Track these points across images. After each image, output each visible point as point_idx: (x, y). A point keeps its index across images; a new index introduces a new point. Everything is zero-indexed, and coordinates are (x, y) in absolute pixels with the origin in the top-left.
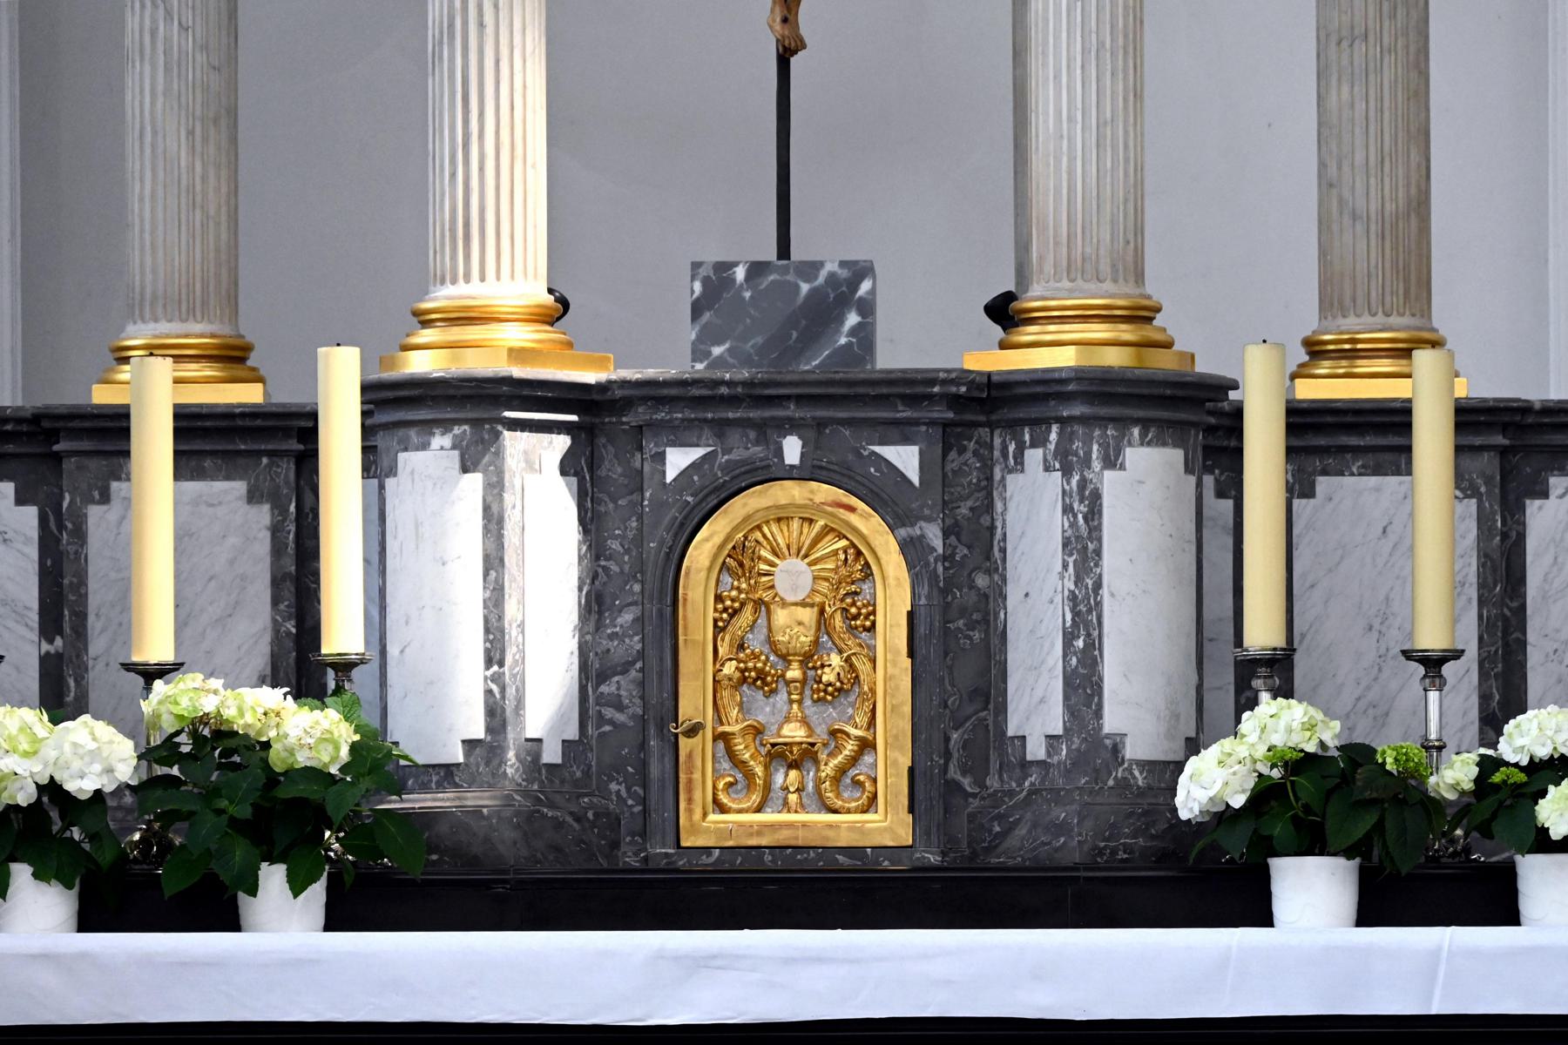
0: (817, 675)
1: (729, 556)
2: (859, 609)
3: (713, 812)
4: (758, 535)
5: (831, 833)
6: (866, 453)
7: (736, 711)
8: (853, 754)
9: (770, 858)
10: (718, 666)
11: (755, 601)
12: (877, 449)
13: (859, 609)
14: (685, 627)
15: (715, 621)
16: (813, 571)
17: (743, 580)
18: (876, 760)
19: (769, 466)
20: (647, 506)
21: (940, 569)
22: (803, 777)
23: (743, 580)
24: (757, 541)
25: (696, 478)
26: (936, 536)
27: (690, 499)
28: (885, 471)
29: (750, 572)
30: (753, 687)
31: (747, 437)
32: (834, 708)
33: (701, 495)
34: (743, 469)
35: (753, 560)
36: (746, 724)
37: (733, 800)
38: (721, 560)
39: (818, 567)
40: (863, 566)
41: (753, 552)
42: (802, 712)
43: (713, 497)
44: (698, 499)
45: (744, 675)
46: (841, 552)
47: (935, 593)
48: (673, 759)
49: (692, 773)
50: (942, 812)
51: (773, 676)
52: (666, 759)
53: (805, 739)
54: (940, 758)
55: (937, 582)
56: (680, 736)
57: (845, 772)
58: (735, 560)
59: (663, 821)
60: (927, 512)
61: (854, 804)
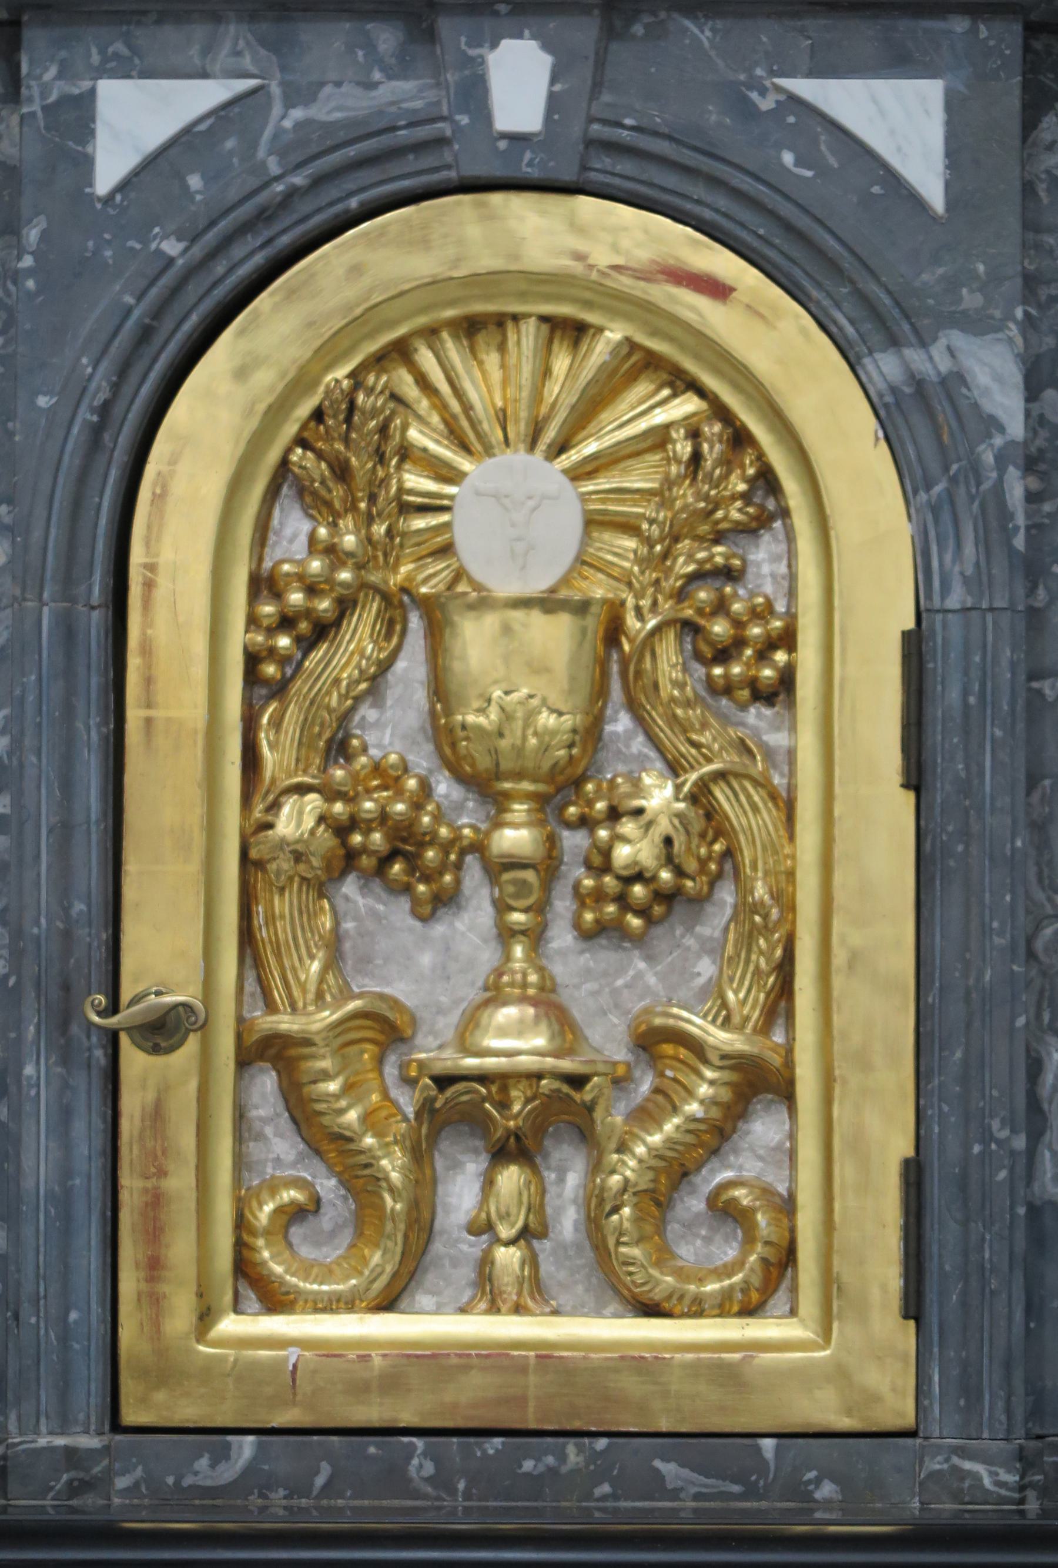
0: (595, 845)
1: (301, 442)
2: (738, 624)
3: (237, 1310)
4: (405, 383)
5: (631, 1385)
6: (766, 104)
7: (315, 966)
8: (715, 1113)
9: (429, 1468)
10: (258, 812)
11: (386, 597)
12: (804, 87)
13: (738, 624)
14: (148, 681)
15: (252, 660)
16: (584, 498)
17: (347, 522)
18: (792, 1136)
19: (441, 142)
20: (30, 272)
21: (1016, 488)
22: (543, 1192)
23: (347, 522)
24: (395, 397)
25: (195, 182)
26: (998, 379)
27: (172, 247)
28: (833, 162)
29: (372, 498)
30: (377, 885)
31: (370, 46)
32: (650, 959)
33: (211, 237)
34: (352, 151)
35: (381, 458)
36: (352, 1005)
37: (306, 1270)
38: (273, 456)
39: (603, 483)
40: (751, 481)
41: (383, 430)
42: (541, 970)
43: (252, 241)
44: (198, 251)
45: (344, 843)
46: (680, 433)
47: (1000, 570)
48: (99, 1125)
49: (162, 1173)
50: (1019, 1315)
51: (446, 848)
52: (79, 1127)
53: (550, 1061)
54: (1014, 1131)
55: (1008, 535)
56: (124, 1040)
57: (685, 1174)
58: (320, 455)
59: (64, 1339)
60: (970, 299)
61: (712, 1287)
